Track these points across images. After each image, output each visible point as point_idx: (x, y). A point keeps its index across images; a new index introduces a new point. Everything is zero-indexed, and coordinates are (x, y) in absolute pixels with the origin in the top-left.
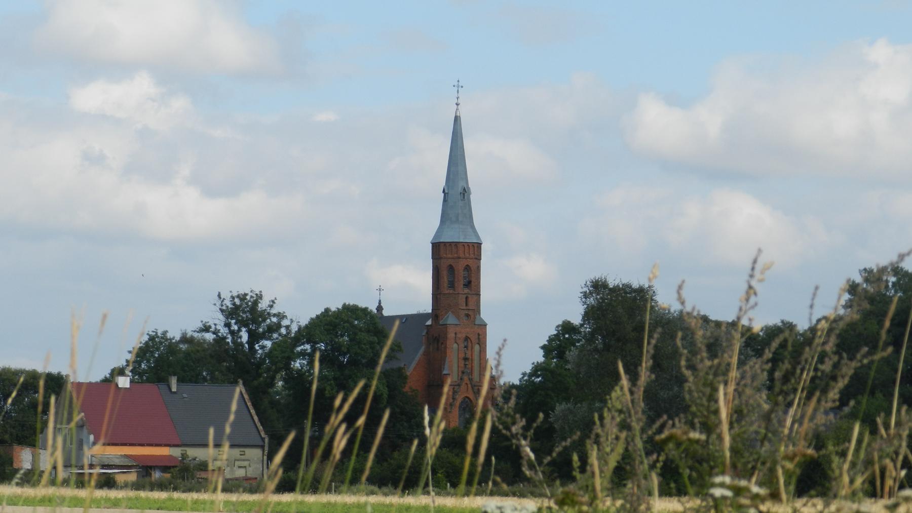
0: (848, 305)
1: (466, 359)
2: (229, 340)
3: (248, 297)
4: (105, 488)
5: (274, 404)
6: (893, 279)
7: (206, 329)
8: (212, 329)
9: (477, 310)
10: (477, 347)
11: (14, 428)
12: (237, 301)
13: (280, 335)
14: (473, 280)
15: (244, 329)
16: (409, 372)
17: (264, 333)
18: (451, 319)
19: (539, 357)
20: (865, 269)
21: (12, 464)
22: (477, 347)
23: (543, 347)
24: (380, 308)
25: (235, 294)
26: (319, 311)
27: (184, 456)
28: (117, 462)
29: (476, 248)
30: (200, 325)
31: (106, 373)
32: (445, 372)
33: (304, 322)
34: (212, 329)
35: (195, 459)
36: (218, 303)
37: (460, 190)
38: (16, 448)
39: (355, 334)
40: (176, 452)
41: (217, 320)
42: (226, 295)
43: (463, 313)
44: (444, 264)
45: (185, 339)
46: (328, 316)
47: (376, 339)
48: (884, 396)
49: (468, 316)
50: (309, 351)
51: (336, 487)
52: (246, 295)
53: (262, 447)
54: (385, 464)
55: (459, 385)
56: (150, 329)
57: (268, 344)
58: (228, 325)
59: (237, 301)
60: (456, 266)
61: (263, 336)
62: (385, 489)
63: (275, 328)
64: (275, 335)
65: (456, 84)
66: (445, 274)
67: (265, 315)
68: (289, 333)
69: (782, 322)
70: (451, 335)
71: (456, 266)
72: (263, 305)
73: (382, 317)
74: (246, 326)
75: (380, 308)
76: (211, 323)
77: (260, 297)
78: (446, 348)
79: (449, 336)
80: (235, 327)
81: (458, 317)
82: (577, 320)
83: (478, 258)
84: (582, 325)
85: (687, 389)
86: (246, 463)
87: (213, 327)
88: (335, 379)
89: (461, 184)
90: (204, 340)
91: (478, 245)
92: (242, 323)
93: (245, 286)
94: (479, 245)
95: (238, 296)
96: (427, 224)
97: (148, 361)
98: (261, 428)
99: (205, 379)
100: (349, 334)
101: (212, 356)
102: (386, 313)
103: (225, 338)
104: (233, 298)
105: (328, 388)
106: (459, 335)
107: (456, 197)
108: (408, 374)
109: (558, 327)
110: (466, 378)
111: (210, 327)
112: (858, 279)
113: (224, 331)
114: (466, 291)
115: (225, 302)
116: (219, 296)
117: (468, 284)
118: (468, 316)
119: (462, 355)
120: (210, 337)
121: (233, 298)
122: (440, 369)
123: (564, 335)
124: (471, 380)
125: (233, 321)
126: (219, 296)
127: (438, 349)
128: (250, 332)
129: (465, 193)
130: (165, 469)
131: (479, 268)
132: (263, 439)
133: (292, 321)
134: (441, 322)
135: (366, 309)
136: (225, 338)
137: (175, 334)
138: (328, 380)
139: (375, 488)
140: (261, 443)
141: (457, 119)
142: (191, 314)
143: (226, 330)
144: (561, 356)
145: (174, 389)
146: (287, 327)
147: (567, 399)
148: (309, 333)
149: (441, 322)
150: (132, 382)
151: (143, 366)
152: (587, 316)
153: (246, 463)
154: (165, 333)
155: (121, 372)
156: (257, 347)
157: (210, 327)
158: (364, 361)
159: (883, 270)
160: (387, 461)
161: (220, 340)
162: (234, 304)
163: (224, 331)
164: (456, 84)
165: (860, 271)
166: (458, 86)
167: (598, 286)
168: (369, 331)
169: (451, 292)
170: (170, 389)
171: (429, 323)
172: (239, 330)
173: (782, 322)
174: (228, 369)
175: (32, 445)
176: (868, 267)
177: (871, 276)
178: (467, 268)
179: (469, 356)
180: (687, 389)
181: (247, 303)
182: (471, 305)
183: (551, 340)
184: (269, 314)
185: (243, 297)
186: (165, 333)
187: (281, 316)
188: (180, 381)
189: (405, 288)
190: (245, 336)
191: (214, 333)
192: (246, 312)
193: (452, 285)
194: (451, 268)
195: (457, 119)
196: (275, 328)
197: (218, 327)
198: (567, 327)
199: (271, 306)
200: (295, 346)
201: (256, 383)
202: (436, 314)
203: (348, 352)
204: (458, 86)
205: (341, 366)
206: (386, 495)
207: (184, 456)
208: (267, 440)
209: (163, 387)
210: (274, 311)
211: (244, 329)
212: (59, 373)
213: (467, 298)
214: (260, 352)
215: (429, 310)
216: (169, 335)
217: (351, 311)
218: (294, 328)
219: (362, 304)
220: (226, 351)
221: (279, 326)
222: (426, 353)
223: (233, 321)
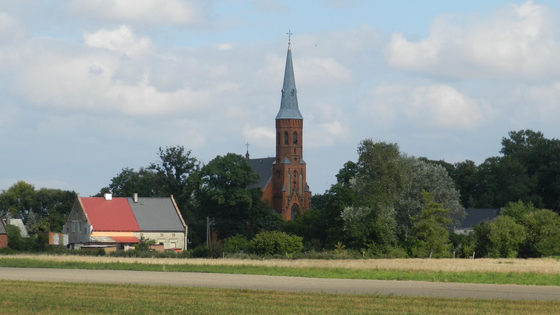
0: (502, 151)
1: (295, 183)
2: (166, 173)
3: (176, 150)
4: (99, 256)
5: (190, 207)
6: (526, 137)
7: (153, 167)
8: (157, 167)
9: (301, 156)
10: (301, 176)
11: (49, 222)
12: (170, 152)
13: (193, 170)
14: (298, 139)
15: (174, 167)
16: (264, 190)
17: (185, 169)
18: (287, 161)
19: (335, 181)
20: (511, 132)
21: (48, 242)
22: (301, 176)
23: (337, 176)
24: (247, 155)
25: (169, 148)
26: (214, 157)
27: (142, 238)
28: (105, 240)
29: (300, 122)
30: (150, 165)
31: (98, 191)
32: (283, 190)
33: (206, 163)
34: (157, 167)
35: (148, 239)
36: (160, 153)
37: (291, 90)
38: (51, 233)
39: (235, 169)
40: (137, 235)
41: (159, 162)
42: (164, 149)
43: (293, 157)
44: (282, 131)
45: (142, 172)
46: (219, 160)
47: (246, 172)
48: (523, 202)
49: (295, 159)
50: (209, 179)
51: (225, 254)
52: (175, 148)
53: (184, 232)
54: (251, 241)
55: (291, 197)
56: (124, 167)
57: (187, 175)
58: (165, 165)
59: (170, 152)
60: (289, 132)
61: (184, 171)
62: (253, 256)
63: (191, 166)
64: (191, 170)
65: (288, 32)
66: (283, 136)
67: (185, 159)
68: (198, 169)
69: (467, 161)
70: (286, 169)
71: (289, 132)
72: (184, 154)
73: (249, 160)
74: (175, 165)
75: (247, 155)
76: (156, 164)
77: (182, 149)
78: (284, 177)
79: (285, 170)
80: (169, 166)
81: (290, 160)
82: (355, 160)
83: (301, 127)
84: (358, 164)
85: (535, 177)
86: (175, 241)
87: (157, 166)
88: (224, 194)
89: (292, 87)
90: (152, 173)
91: (301, 120)
92: (173, 164)
93: (174, 143)
94: (302, 120)
95: (170, 149)
96: (274, 108)
97: (122, 185)
98: (183, 221)
99: (152, 194)
100: (232, 170)
101: (156, 182)
102: (251, 157)
103: (163, 172)
104: (168, 150)
105: (220, 199)
106: (291, 170)
107: (289, 94)
108: (263, 191)
109: (345, 164)
110: (295, 193)
111: (155, 166)
112: (508, 137)
113: (163, 168)
114: (295, 145)
115: (163, 152)
116: (160, 149)
117: (296, 142)
118: (295, 159)
119: (293, 180)
120: (155, 171)
121: (168, 150)
122: (281, 188)
123: (348, 169)
124: (298, 194)
125: (168, 163)
126: (160, 149)
127: (279, 177)
128: (177, 169)
129: (294, 92)
130: (131, 244)
131: (301, 133)
132: (185, 228)
133: (200, 162)
134: (281, 163)
135: (240, 156)
136: (163, 172)
137: (137, 170)
138: (220, 195)
139: (247, 255)
140: (184, 230)
141: (289, 52)
142: (145, 158)
143: (164, 168)
144: (347, 181)
145: (136, 201)
146: (197, 166)
147: (350, 205)
148: (207, 170)
149: (281, 163)
150: (112, 197)
151: (119, 188)
152: (360, 159)
153: (175, 241)
154: (132, 169)
155: (105, 191)
156: (181, 177)
157: (155, 166)
158: (239, 184)
159: (521, 132)
160: (252, 239)
161: (161, 173)
162: (168, 154)
163: (163, 168)
164: (288, 32)
165: (509, 133)
166: (290, 34)
167: (367, 144)
168: (241, 168)
169: (287, 146)
170: (134, 200)
171: (275, 163)
172: (171, 168)
173: (467, 161)
174: (165, 189)
175: (59, 232)
176: (513, 130)
177: (517, 136)
178: (295, 133)
179: (296, 181)
180: (535, 177)
181: (175, 153)
182: (298, 154)
183: (341, 171)
184: (187, 159)
185: (173, 150)
186: (132, 169)
187: (194, 160)
188: (139, 196)
189: (262, 143)
190: (174, 171)
191: (157, 169)
192: (175, 158)
193: (287, 142)
194: (286, 133)
195: (289, 52)
196: (191, 166)
197: (160, 166)
198: (350, 165)
199: (188, 155)
200: (201, 176)
201: (181, 196)
202: (278, 158)
203: (231, 179)
204: (290, 34)
205: (227, 187)
206: (252, 259)
207: (142, 238)
208: (187, 228)
209: (130, 199)
210: (190, 157)
211: (174, 167)
212: (73, 191)
213: (295, 149)
214: (183, 179)
215: (274, 155)
216: (134, 171)
217: (232, 157)
218: (201, 166)
219: (238, 153)
220: (164, 179)
221: (192, 165)
222: (273, 180)
223: (168, 163)
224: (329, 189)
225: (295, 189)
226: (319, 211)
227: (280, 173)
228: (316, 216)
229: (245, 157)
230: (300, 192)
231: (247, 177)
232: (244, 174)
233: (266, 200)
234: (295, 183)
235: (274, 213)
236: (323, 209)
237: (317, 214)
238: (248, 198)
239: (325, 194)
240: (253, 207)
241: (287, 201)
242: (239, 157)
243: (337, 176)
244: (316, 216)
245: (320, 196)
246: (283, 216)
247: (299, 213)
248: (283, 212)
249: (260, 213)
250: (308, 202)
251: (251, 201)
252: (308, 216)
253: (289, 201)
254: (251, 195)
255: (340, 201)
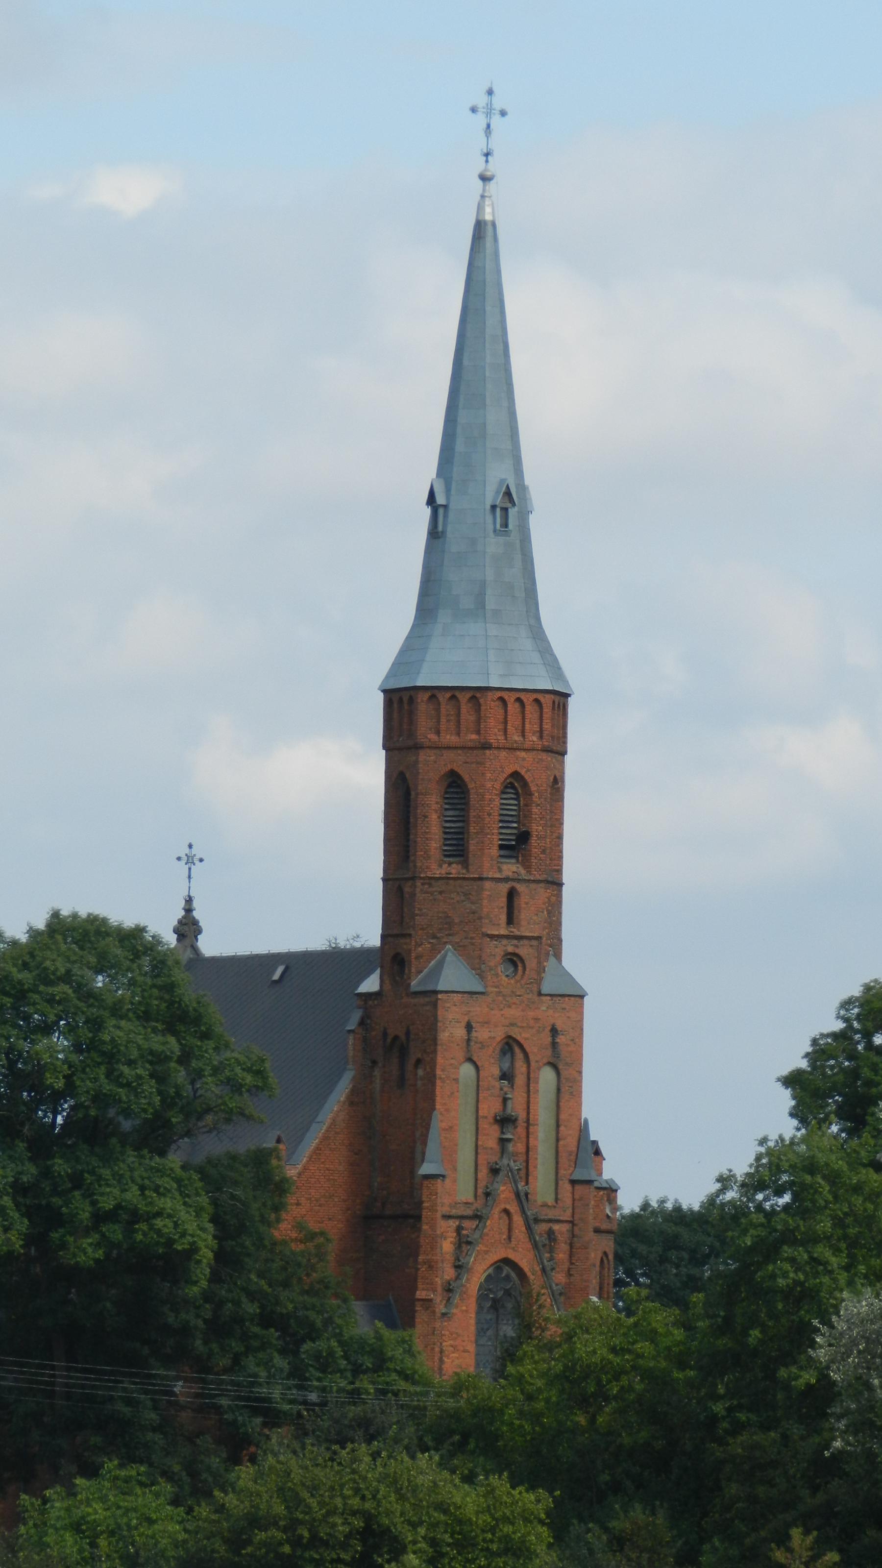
10: (546, 1077)
14: (536, 829)
18: (453, 975)
19: (776, 1119)
23: (792, 1080)
24: (188, 928)
32: (426, 1169)
37: (491, 495)
43: (496, 951)
44: (430, 769)
49: (514, 960)
54: (204, 1510)
60: (470, 779)
65: (482, 101)
70: (451, 1031)
71: (470, 779)
75: (188, 928)
78: (431, 1079)
79: (443, 1036)
81: (478, 967)
89: (497, 473)
94: (560, 699)
96: (372, 622)
102: (210, 945)
106: (481, 1034)
107: (476, 519)
108: (292, 1172)
109: (847, 1004)
110: (504, 1190)
114: (510, 868)
117: (517, 845)
118: (514, 960)
119: (491, 1107)
122: (412, 1155)
124: (522, 1198)
127: (402, 1081)
129: (509, 505)
131: (557, 785)
134: (415, 984)
141: (482, 233)
149: (415, 984)
158: (127, 1125)
160: (208, 1495)
164: (482, 101)
166: (489, 110)
168: (146, 1017)
169: (455, 870)
171: (371, 984)
178: (516, 784)
179: (517, 1107)
182: (530, 922)
183: (820, 1052)
193: (457, 847)
194: (455, 786)
195: (482, 233)
203: (70, 1089)
204: (489, 110)
205: (43, 1144)
213: (512, 895)
215: (372, 937)
219: (122, 914)
222: (358, 1098)
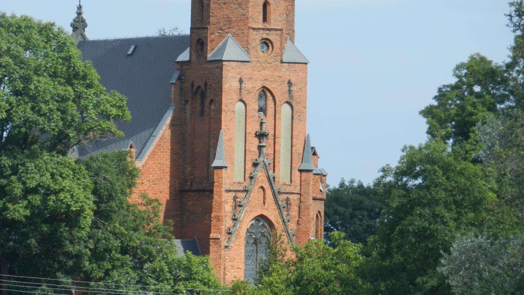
18: (232, 51)
19: (418, 134)
22: (285, 109)
23: (428, 112)
24: (79, 24)
32: (216, 163)
39: (26, 80)
49: (266, 43)
73: (84, 44)
75: (79, 24)
78: (219, 111)
79: (226, 86)
81: (246, 47)
82: (499, 55)
84: (510, 66)
106: (247, 85)
108: (139, 164)
109: (458, 68)
118: (266, 43)
119: (254, 128)
124: (271, 181)
134: (210, 56)
144: (463, 130)
168: (54, 75)
171: (184, 56)
179: (268, 128)
182: (276, 19)
183: (442, 96)
198: (479, 73)
202: (198, 39)
219: (41, 16)
224: (394, 163)
225: (260, 163)
226: (353, 249)
227: (203, 96)
228: (343, 267)
229: (69, 30)
230: (282, 174)
231: (73, 109)
232: (64, 99)
233: (150, 202)
234: (261, 136)
235: (178, 250)
236: (371, 239)
237: (347, 260)
238: (77, 194)
239: (377, 184)
240: (95, 225)
241: (228, 208)
242: (46, 30)
243: (428, 112)
244: (343, 267)
245: (361, 190)
246: (211, 265)
247: (273, 253)
248: (213, 248)
249: (124, 251)
250: (313, 214)
251: (89, 205)
252: (313, 267)
253: (238, 206)
254: (88, 181)
255: (440, 209)
